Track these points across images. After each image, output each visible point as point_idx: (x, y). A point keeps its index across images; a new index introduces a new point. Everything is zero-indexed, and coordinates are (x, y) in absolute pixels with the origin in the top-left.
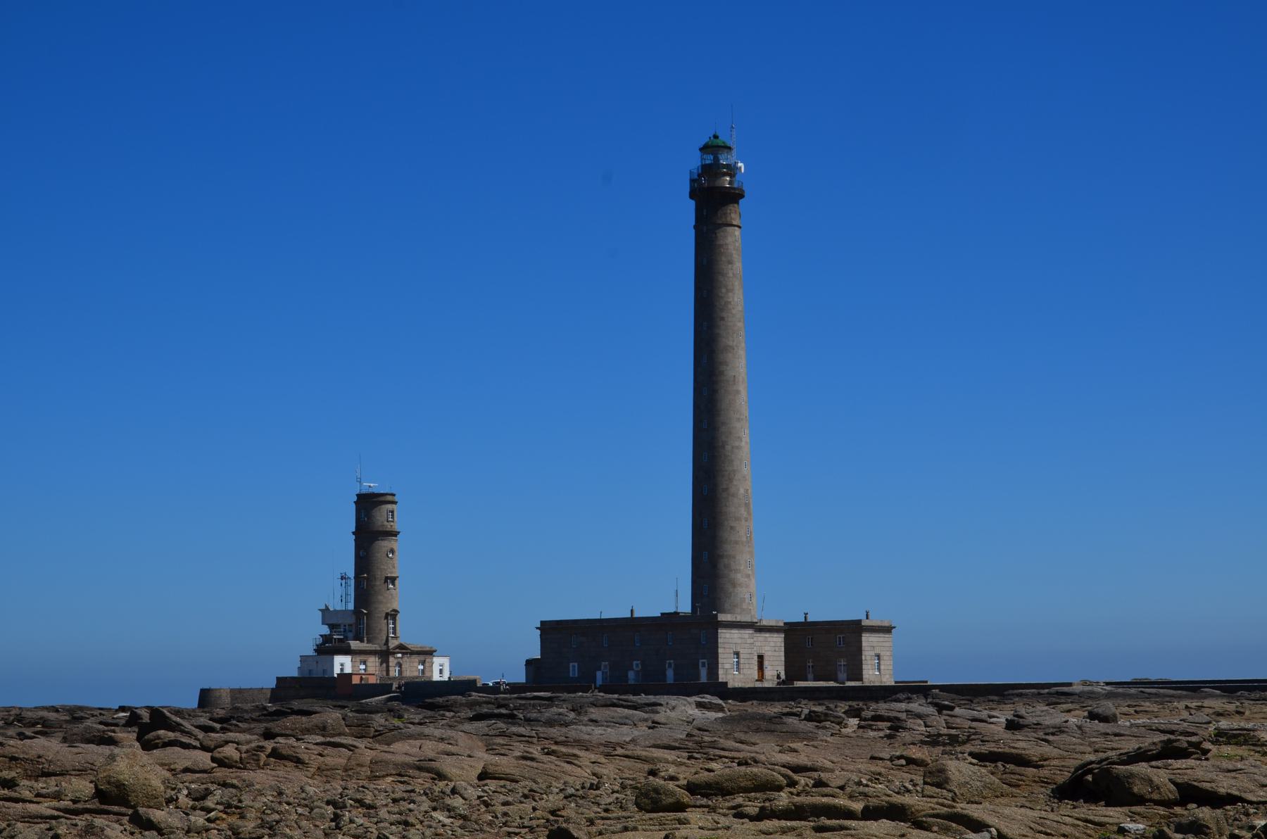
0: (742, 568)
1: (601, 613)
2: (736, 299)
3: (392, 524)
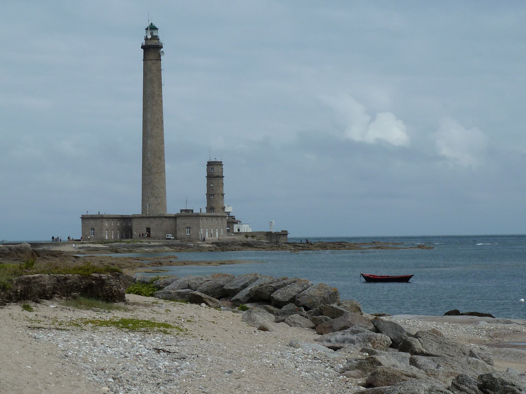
3: (213, 173)
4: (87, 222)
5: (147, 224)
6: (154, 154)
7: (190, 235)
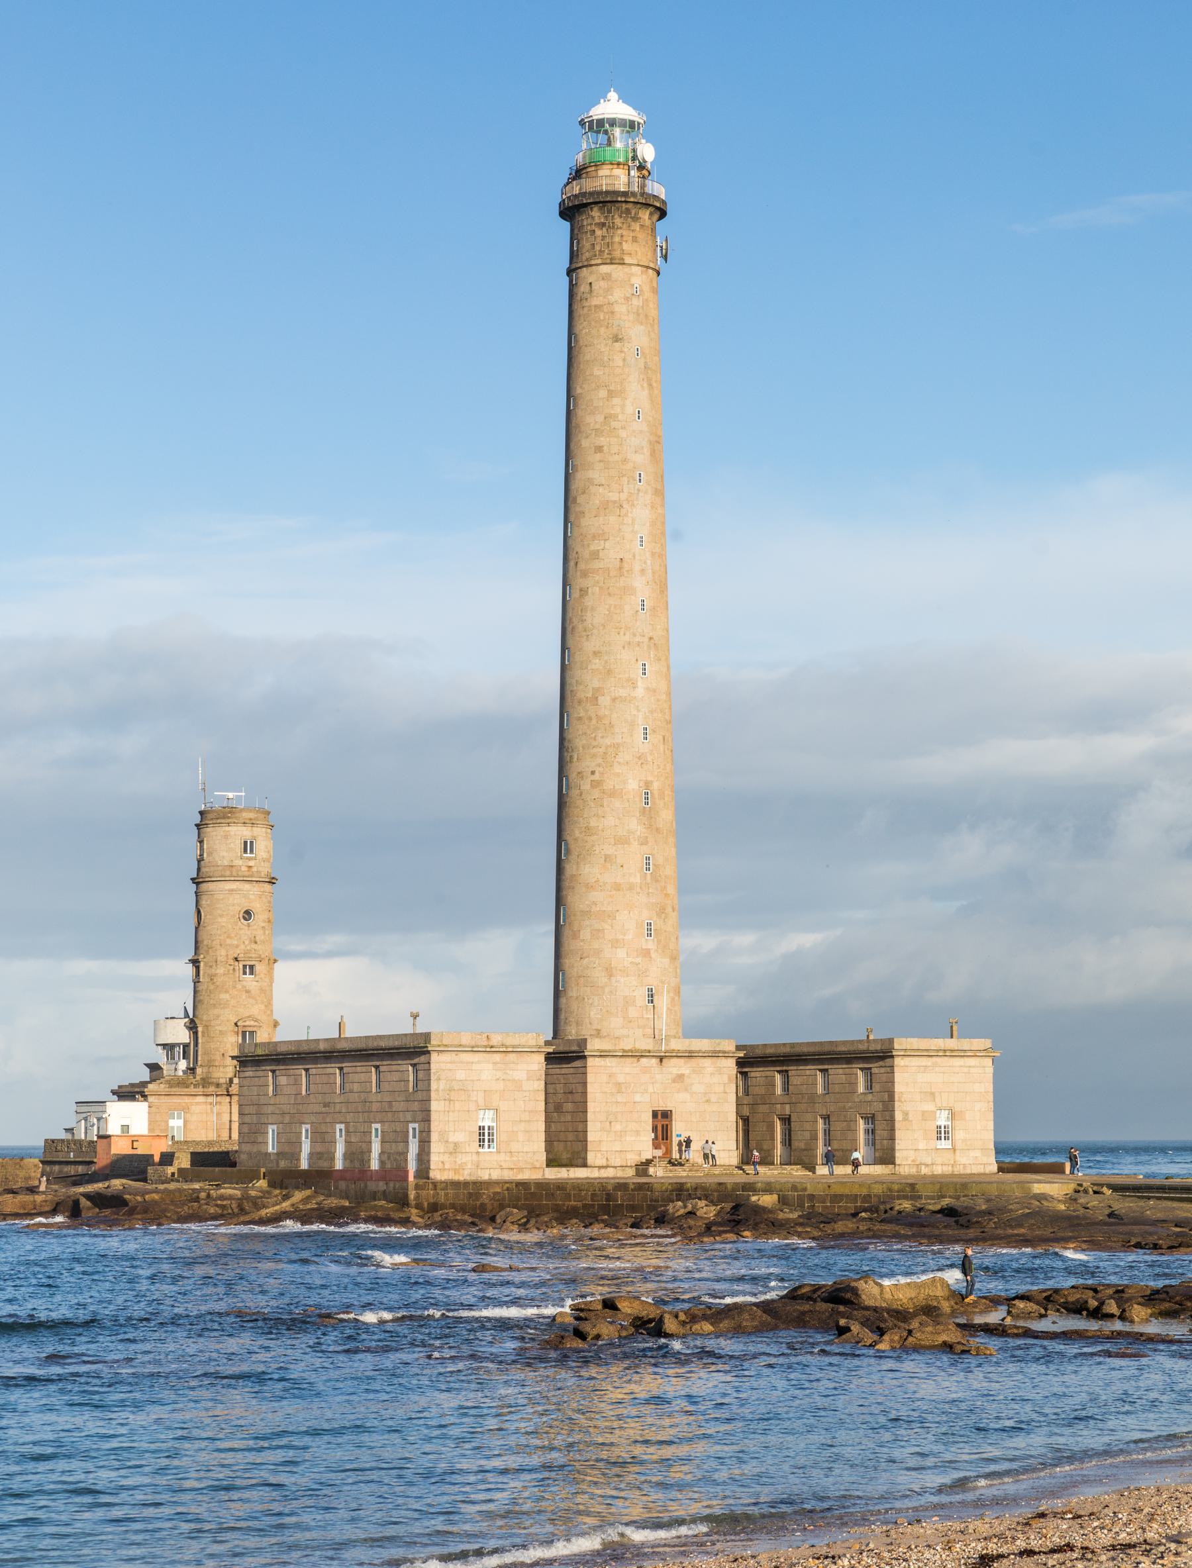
0: (629, 937)
1: (308, 1028)
7: (954, 1150)
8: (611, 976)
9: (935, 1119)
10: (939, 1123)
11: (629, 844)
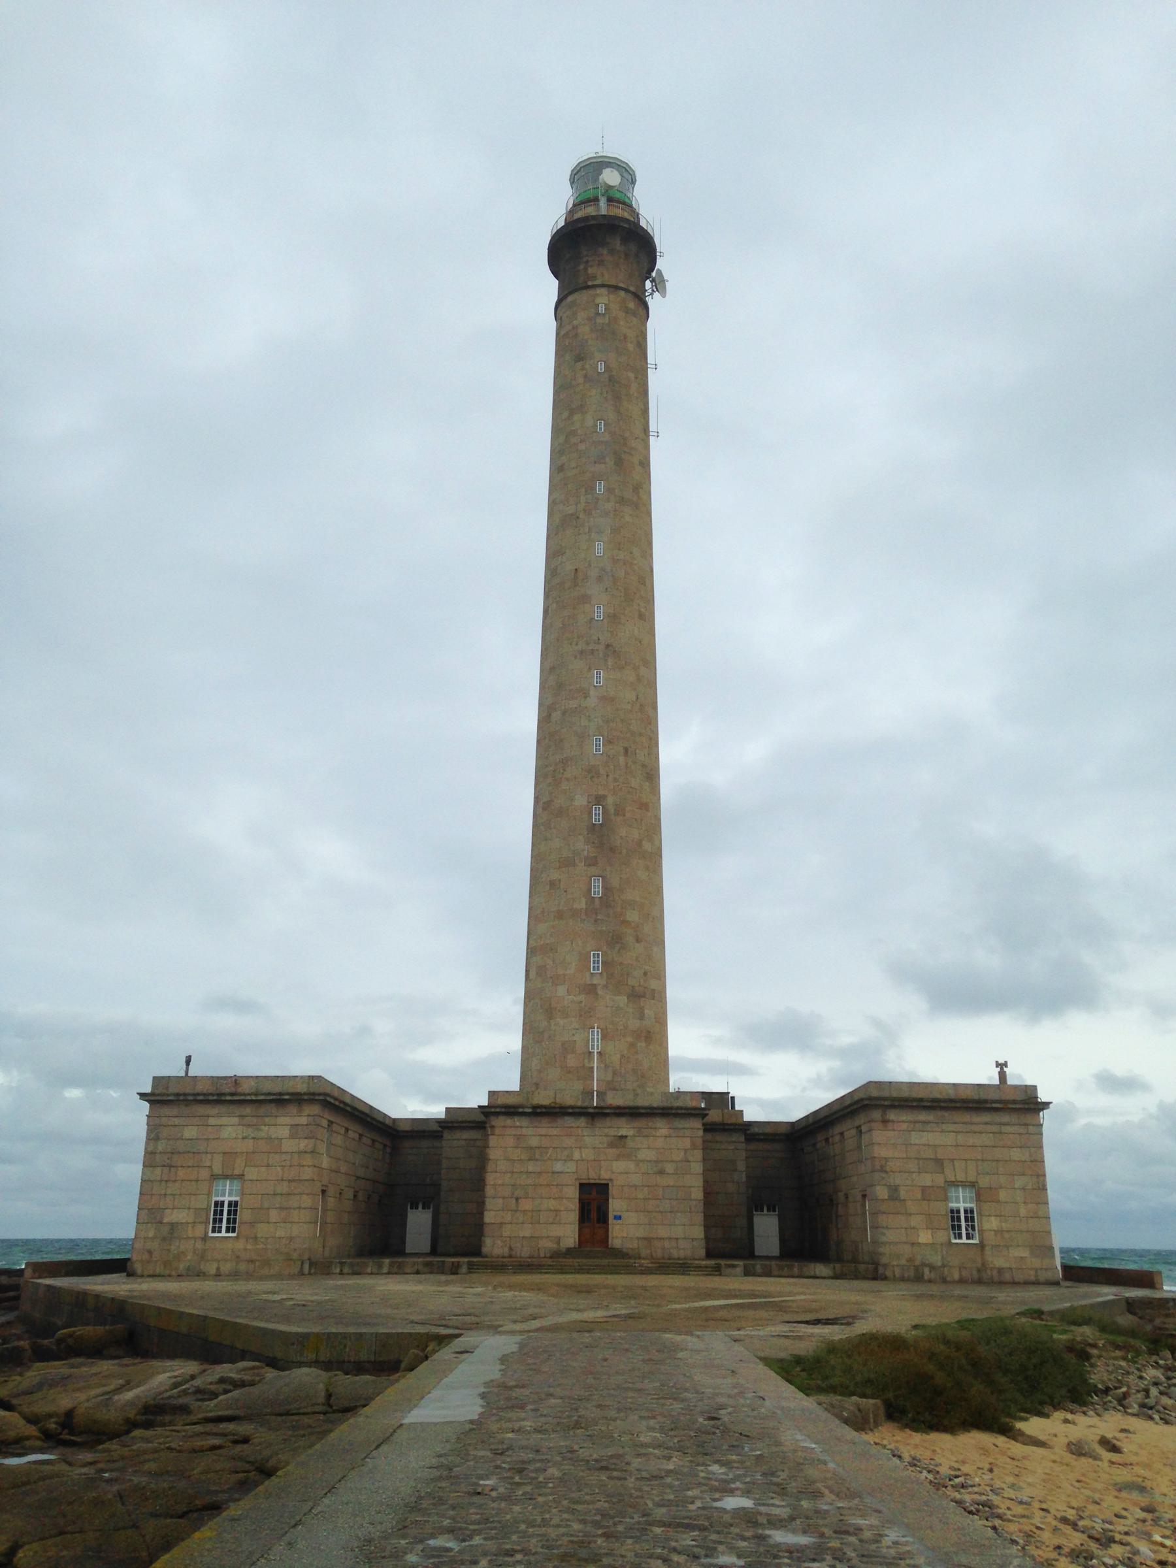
2: (589, 422)
4: (190, 1132)
5: (588, 1154)
6: (626, 750)
7: (982, 1246)
8: (551, 1018)
9: (946, 1199)
10: (954, 1205)
11: (574, 865)
